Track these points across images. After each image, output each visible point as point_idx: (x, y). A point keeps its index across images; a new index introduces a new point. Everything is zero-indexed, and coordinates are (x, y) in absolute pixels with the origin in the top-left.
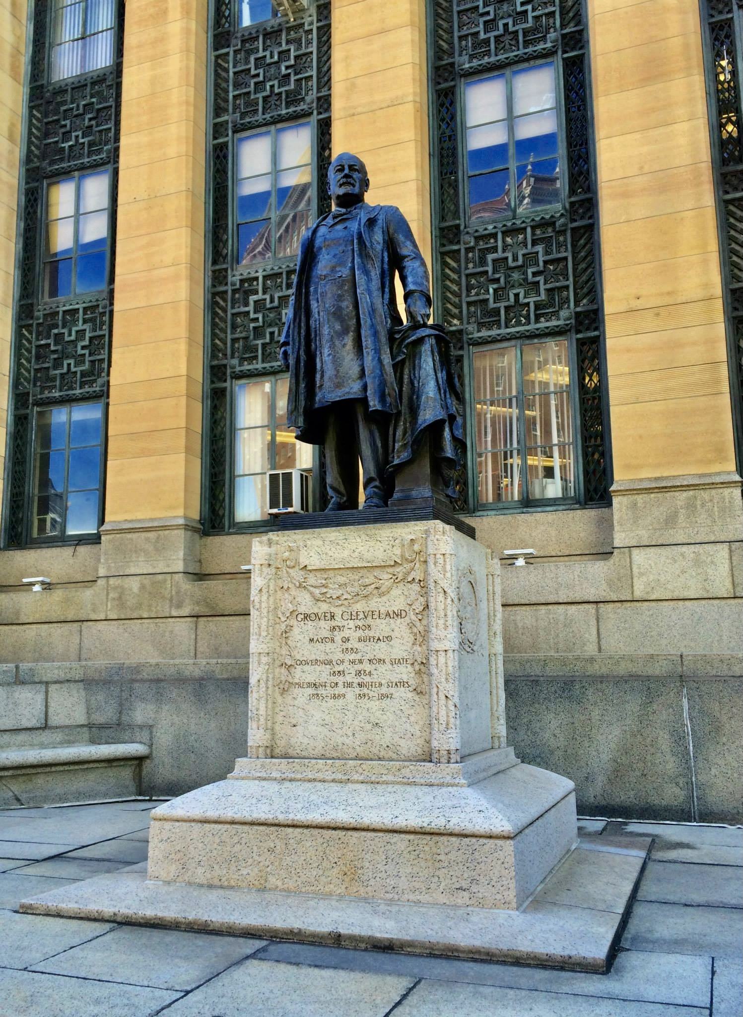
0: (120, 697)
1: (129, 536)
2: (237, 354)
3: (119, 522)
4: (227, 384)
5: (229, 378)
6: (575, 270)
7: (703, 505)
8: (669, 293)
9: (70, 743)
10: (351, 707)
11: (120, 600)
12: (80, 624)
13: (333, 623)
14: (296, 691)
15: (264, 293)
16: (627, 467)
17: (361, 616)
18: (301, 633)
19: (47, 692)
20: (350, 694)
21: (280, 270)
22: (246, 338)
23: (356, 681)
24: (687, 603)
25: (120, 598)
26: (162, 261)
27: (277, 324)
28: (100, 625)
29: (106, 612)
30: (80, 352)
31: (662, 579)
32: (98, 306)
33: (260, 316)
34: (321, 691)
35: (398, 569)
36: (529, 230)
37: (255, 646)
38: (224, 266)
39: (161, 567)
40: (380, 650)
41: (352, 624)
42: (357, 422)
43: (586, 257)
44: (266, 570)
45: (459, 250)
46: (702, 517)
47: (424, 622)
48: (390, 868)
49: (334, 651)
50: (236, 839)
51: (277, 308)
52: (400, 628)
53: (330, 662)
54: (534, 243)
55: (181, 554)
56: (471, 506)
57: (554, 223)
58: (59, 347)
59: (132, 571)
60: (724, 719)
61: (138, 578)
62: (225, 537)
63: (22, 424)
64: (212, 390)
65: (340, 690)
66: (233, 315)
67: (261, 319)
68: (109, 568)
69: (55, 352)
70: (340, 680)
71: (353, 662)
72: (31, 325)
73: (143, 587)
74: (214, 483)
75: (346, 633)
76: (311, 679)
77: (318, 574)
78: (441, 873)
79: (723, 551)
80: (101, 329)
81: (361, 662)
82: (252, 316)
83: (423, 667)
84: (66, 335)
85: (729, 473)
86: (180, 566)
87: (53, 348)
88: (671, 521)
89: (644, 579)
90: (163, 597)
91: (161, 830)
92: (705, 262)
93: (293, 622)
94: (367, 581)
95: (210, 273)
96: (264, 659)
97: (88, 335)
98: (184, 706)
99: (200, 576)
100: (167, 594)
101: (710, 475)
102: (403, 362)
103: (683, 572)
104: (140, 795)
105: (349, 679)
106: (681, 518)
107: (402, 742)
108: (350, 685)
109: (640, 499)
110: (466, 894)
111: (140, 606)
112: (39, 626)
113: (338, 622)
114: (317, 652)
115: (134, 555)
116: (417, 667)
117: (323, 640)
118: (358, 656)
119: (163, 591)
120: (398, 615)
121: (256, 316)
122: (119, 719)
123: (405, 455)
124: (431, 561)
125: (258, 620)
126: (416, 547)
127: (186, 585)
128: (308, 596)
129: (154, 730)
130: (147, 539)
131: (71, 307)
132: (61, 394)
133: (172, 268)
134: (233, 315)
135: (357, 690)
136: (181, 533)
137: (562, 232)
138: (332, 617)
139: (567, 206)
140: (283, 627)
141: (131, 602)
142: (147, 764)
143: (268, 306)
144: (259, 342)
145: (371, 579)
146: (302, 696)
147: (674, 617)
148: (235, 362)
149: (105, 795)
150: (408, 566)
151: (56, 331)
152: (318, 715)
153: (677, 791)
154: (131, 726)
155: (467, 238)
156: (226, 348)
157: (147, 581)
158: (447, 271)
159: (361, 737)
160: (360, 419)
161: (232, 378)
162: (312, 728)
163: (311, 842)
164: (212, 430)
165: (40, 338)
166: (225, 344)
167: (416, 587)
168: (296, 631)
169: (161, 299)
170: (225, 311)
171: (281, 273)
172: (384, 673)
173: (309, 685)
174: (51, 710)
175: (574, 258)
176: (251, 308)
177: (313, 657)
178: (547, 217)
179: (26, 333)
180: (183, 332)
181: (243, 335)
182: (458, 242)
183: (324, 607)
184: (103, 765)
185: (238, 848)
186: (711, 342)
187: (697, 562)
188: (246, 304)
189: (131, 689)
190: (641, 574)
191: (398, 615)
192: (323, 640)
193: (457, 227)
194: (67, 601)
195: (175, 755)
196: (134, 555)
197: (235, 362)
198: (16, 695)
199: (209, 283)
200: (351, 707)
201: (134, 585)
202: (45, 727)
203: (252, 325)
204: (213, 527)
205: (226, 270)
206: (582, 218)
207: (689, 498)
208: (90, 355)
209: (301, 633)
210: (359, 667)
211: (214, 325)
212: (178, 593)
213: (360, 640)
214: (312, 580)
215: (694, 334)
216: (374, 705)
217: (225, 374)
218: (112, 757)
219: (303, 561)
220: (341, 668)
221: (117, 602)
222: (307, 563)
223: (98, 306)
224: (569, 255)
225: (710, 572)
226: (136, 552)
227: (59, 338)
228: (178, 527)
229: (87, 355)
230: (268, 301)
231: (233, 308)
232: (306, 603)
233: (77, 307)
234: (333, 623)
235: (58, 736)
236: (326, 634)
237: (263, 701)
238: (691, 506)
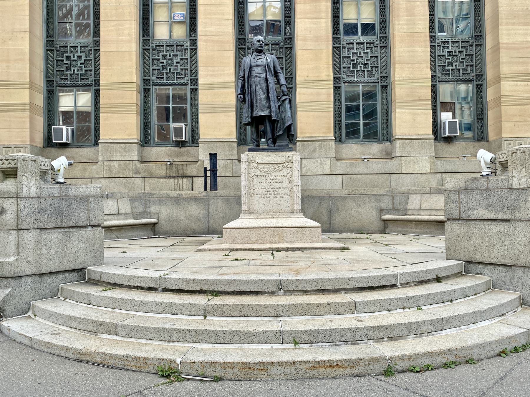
0: (145, 204)
1: (113, 145)
2: (154, 76)
3: (107, 139)
4: (151, 87)
5: (151, 85)
6: (285, 62)
7: (324, 146)
8: (317, 76)
9: (127, 219)
10: (272, 200)
11: (110, 170)
12: (91, 179)
13: (266, 178)
14: (256, 196)
15: (166, 52)
16: (301, 133)
17: (274, 176)
18: (256, 180)
19: (118, 201)
20: (271, 197)
21: (173, 44)
22: (158, 70)
23: (273, 193)
24: (318, 176)
25: (109, 169)
26: (123, 33)
28: (100, 180)
29: (103, 174)
30: (79, 65)
31: (311, 168)
32: (88, 46)
34: (263, 196)
35: (284, 164)
36: (270, 45)
37: (243, 184)
38: (148, 38)
39: (127, 158)
40: (280, 185)
41: (271, 178)
42: (266, 121)
43: (289, 58)
44: (247, 163)
45: (245, 48)
46: (323, 150)
47: (292, 178)
48: (291, 236)
49: (267, 185)
50: (249, 232)
51: (172, 59)
52: (285, 180)
53: (265, 188)
54: (272, 50)
55: (136, 153)
56: (248, 142)
57: (279, 44)
58: (69, 62)
59: (115, 159)
60: (340, 206)
61: (118, 162)
62: (152, 148)
63: (51, 94)
64: (144, 89)
65: (268, 195)
66: (153, 59)
67: (165, 62)
68: (103, 158)
69: (66, 64)
70: (268, 193)
71: (272, 188)
72: (53, 50)
73: (120, 165)
74: (146, 126)
75: (270, 181)
76: (260, 193)
77: (261, 165)
78: (304, 236)
79: (328, 161)
80: (89, 57)
81: (274, 188)
82: (161, 61)
83: (291, 190)
84: (72, 57)
85: (331, 137)
86: (136, 158)
87: (65, 62)
88: (314, 151)
89: (305, 168)
90: (129, 170)
91: (226, 231)
92: (328, 68)
93: (254, 177)
94: (276, 167)
95: (142, 40)
96: (247, 187)
97: (83, 58)
98: (171, 206)
99: (142, 162)
100: (131, 168)
101: (326, 137)
102: (280, 105)
103: (317, 166)
104: (155, 236)
105: (271, 193)
106: (317, 150)
107: (286, 208)
108: (271, 194)
109: (305, 143)
110: (310, 240)
111: (119, 172)
112: (71, 180)
113: (267, 178)
114: (262, 185)
115: (115, 153)
116: (290, 190)
117: (263, 183)
118: (273, 187)
119: (129, 167)
120: (285, 176)
121: (163, 61)
122: (145, 211)
123: (281, 133)
124: (294, 162)
125: (244, 177)
126: (290, 158)
127: (139, 165)
128: (258, 171)
129: (160, 214)
130: (121, 147)
131: (74, 45)
132: (71, 83)
133: (129, 37)
134: (153, 59)
135: (273, 196)
136: (136, 146)
137: (282, 48)
138: (266, 176)
139: (284, 39)
140: (251, 179)
141: (115, 171)
142: (157, 226)
143: (168, 58)
144: (165, 72)
145: (277, 167)
146: (257, 197)
147: (313, 180)
148: (154, 78)
149: (144, 236)
150: (288, 163)
151: (67, 54)
152: (262, 202)
153: (327, 225)
154: (150, 213)
155: (248, 44)
156: (150, 73)
157: (122, 163)
158: (240, 55)
159: (274, 207)
160: (267, 120)
161: (153, 85)
162: (260, 206)
163: (270, 231)
164: (144, 105)
165: (58, 56)
166: (149, 71)
167: (289, 169)
168: (255, 180)
169: (123, 50)
170: (149, 58)
171: (174, 45)
172: (281, 191)
173: (259, 194)
174: (119, 208)
175: (285, 58)
176: (160, 57)
177: (260, 187)
178: (277, 41)
179: (50, 53)
180: (134, 65)
181: (157, 68)
182: (245, 45)
183: (263, 174)
184: (143, 226)
185: (250, 234)
186: (329, 94)
187: (321, 164)
188: (159, 56)
189: (149, 201)
190: (305, 167)
191: (285, 176)
192: (263, 183)
193: (245, 39)
194: (84, 170)
195: (168, 222)
196: (115, 153)
197: (154, 78)
198: (108, 202)
199: (142, 44)
200: (272, 200)
201: (116, 164)
202: (118, 214)
203: (161, 65)
204: (146, 143)
205: (149, 40)
206: (288, 44)
207: (319, 144)
208: (85, 67)
209: (256, 180)
210: (274, 190)
211: (144, 63)
212: (136, 168)
213: (274, 182)
214: (260, 166)
215: (324, 91)
216: (278, 199)
217: (149, 83)
218: (147, 223)
219: (257, 161)
220: (269, 190)
221: (108, 171)
222: (258, 161)
223: (88, 46)
224: (284, 56)
225: (325, 167)
226: (116, 151)
227: (68, 57)
228: (134, 143)
229: (83, 67)
230: (168, 56)
231: (152, 56)
232: (258, 173)
233: (77, 45)
234: (266, 178)
235: (123, 217)
236: (264, 181)
237: (247, 199)
238: (320, 146)
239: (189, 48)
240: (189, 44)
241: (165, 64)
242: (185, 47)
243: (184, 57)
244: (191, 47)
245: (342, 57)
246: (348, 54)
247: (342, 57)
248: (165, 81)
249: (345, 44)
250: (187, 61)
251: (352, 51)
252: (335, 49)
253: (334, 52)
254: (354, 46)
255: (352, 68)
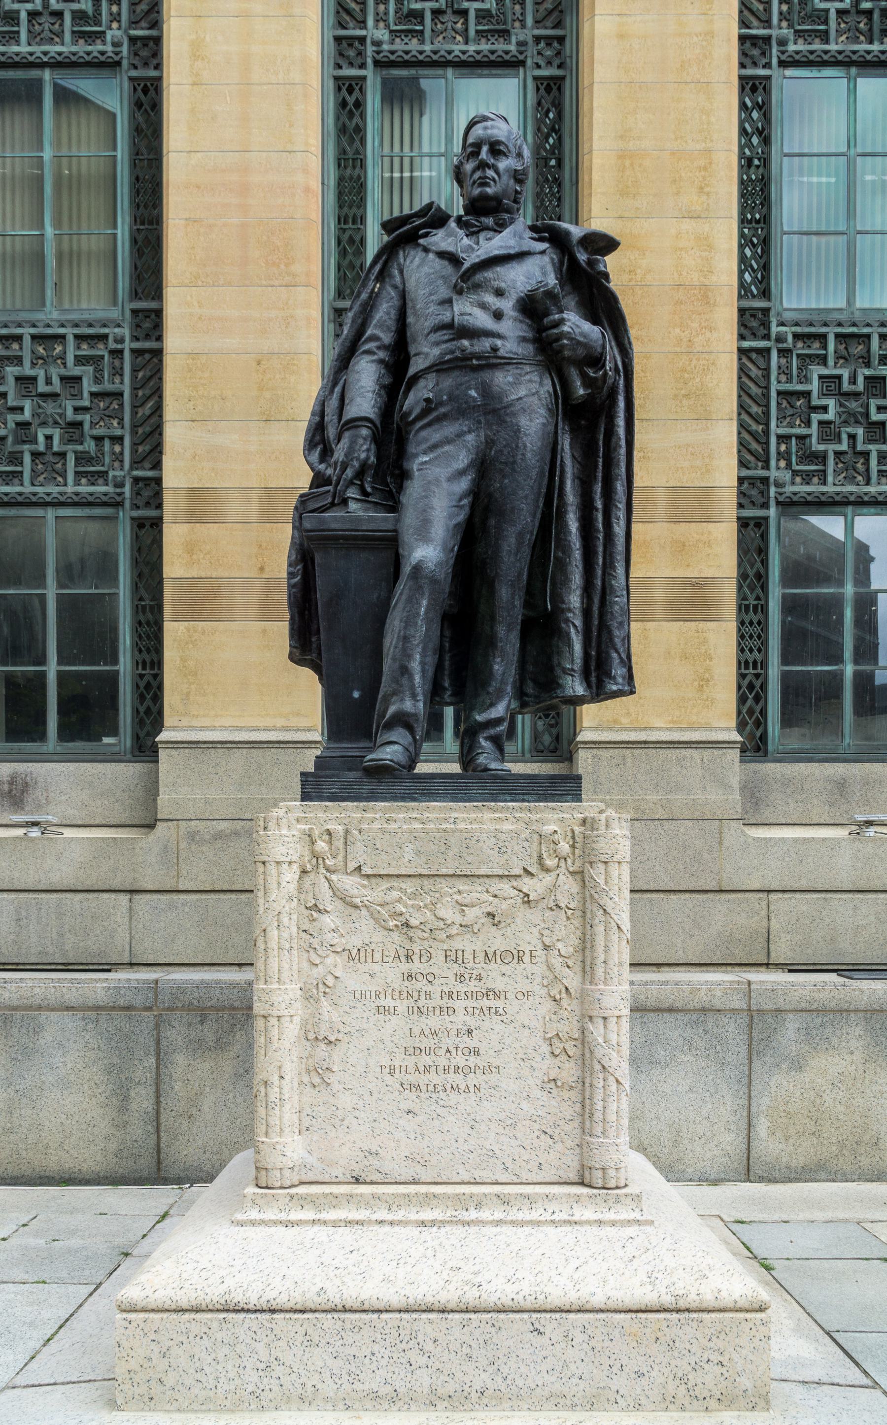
27: (56, 423)
33: (28, 405)
239: (127, 346)
240: (126, 332)
241: (27, 415)
242: (112, 345)
243: (107, 386)
244: (137, 345)
245: (773, 394)
246: (805, 379)
247: (773, 394)
248: (28, 489)
249: (790, 338)
250: (121, 405)
251: (816, 371)
252: (745, 360)
253: (742, 371)
254: (825, 347)
255: (814, 439)
